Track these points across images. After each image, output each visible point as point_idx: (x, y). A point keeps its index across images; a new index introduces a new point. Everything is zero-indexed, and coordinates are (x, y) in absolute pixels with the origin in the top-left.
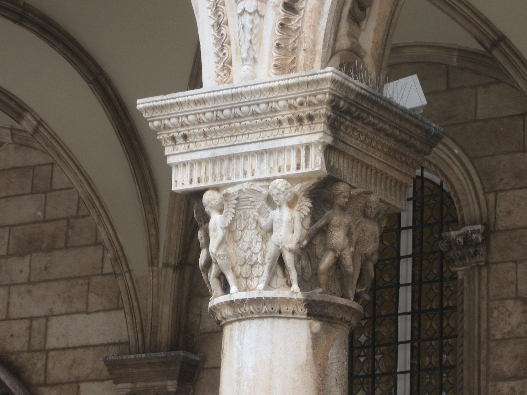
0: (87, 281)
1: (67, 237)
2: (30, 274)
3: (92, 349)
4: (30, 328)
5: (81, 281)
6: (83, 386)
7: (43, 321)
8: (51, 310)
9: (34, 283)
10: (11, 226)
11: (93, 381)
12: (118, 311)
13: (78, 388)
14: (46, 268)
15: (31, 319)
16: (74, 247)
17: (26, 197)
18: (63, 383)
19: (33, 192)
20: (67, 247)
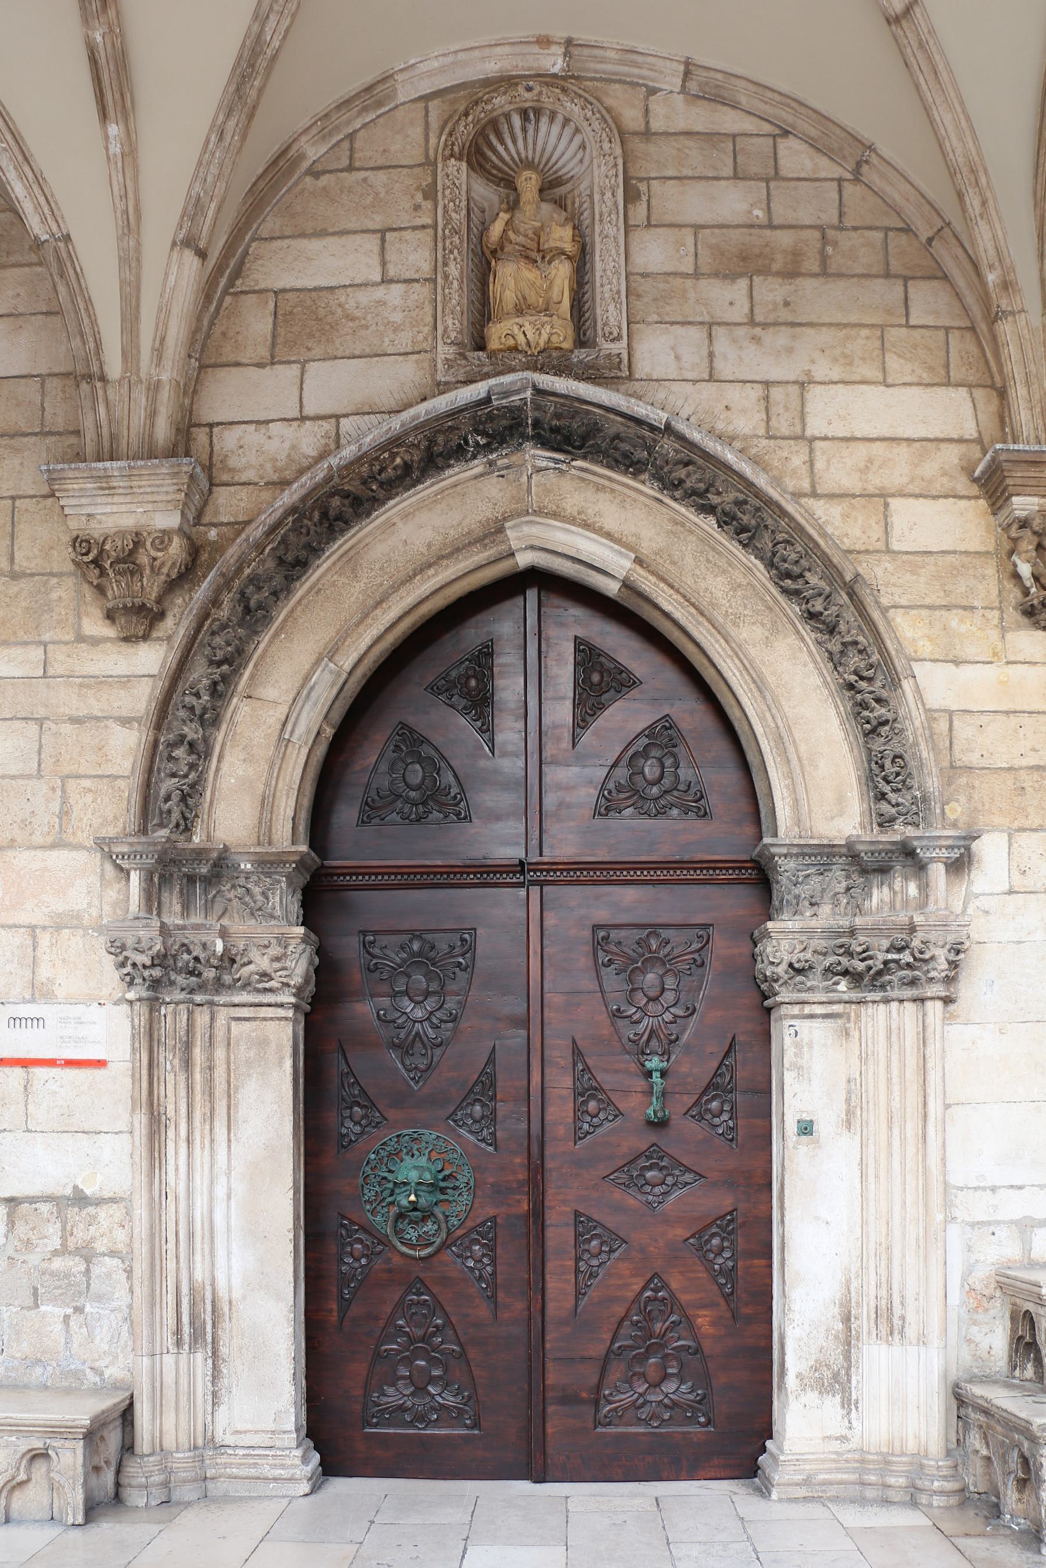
0: (879, 333)
1: (824, 259)
2: (752, 310)
3: (904, 444)
4: (767, 398)
5: (865, 332)
6: (895, 503)
7: (794, 390)
8: (808, 373)
9: (765, 326)
10: (697, 228)
11: (917, 496)
12: (950, 388)
13: (886, 505)
14: (787, 304)
15: (767, 384)
16: (840, 275)
17: (723, 183)
18: (854, 496)
19: (736, 177)
20: (824, 272)
